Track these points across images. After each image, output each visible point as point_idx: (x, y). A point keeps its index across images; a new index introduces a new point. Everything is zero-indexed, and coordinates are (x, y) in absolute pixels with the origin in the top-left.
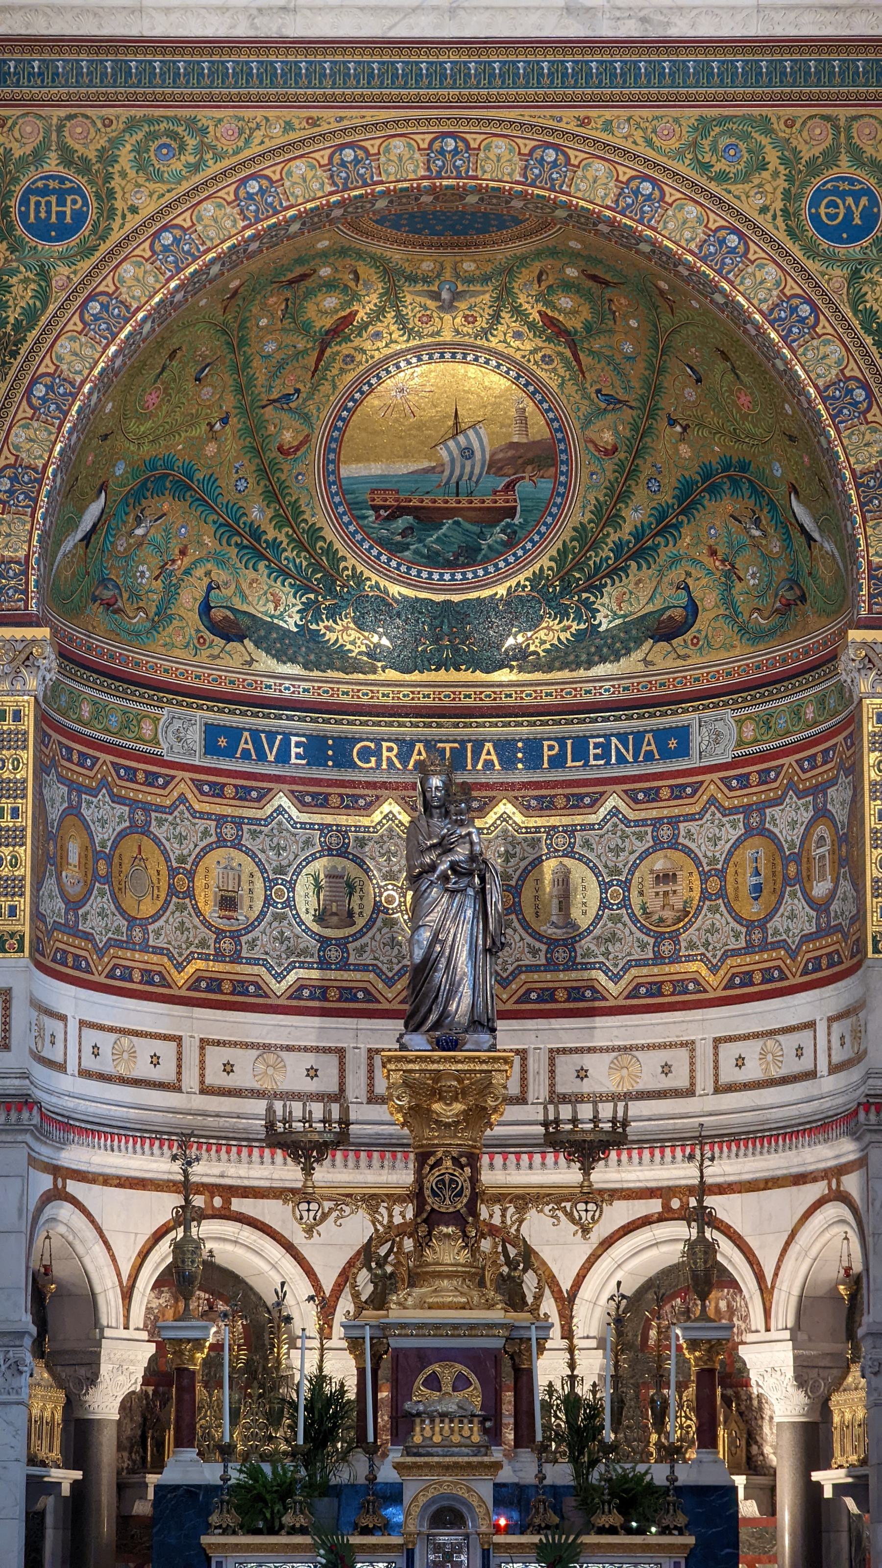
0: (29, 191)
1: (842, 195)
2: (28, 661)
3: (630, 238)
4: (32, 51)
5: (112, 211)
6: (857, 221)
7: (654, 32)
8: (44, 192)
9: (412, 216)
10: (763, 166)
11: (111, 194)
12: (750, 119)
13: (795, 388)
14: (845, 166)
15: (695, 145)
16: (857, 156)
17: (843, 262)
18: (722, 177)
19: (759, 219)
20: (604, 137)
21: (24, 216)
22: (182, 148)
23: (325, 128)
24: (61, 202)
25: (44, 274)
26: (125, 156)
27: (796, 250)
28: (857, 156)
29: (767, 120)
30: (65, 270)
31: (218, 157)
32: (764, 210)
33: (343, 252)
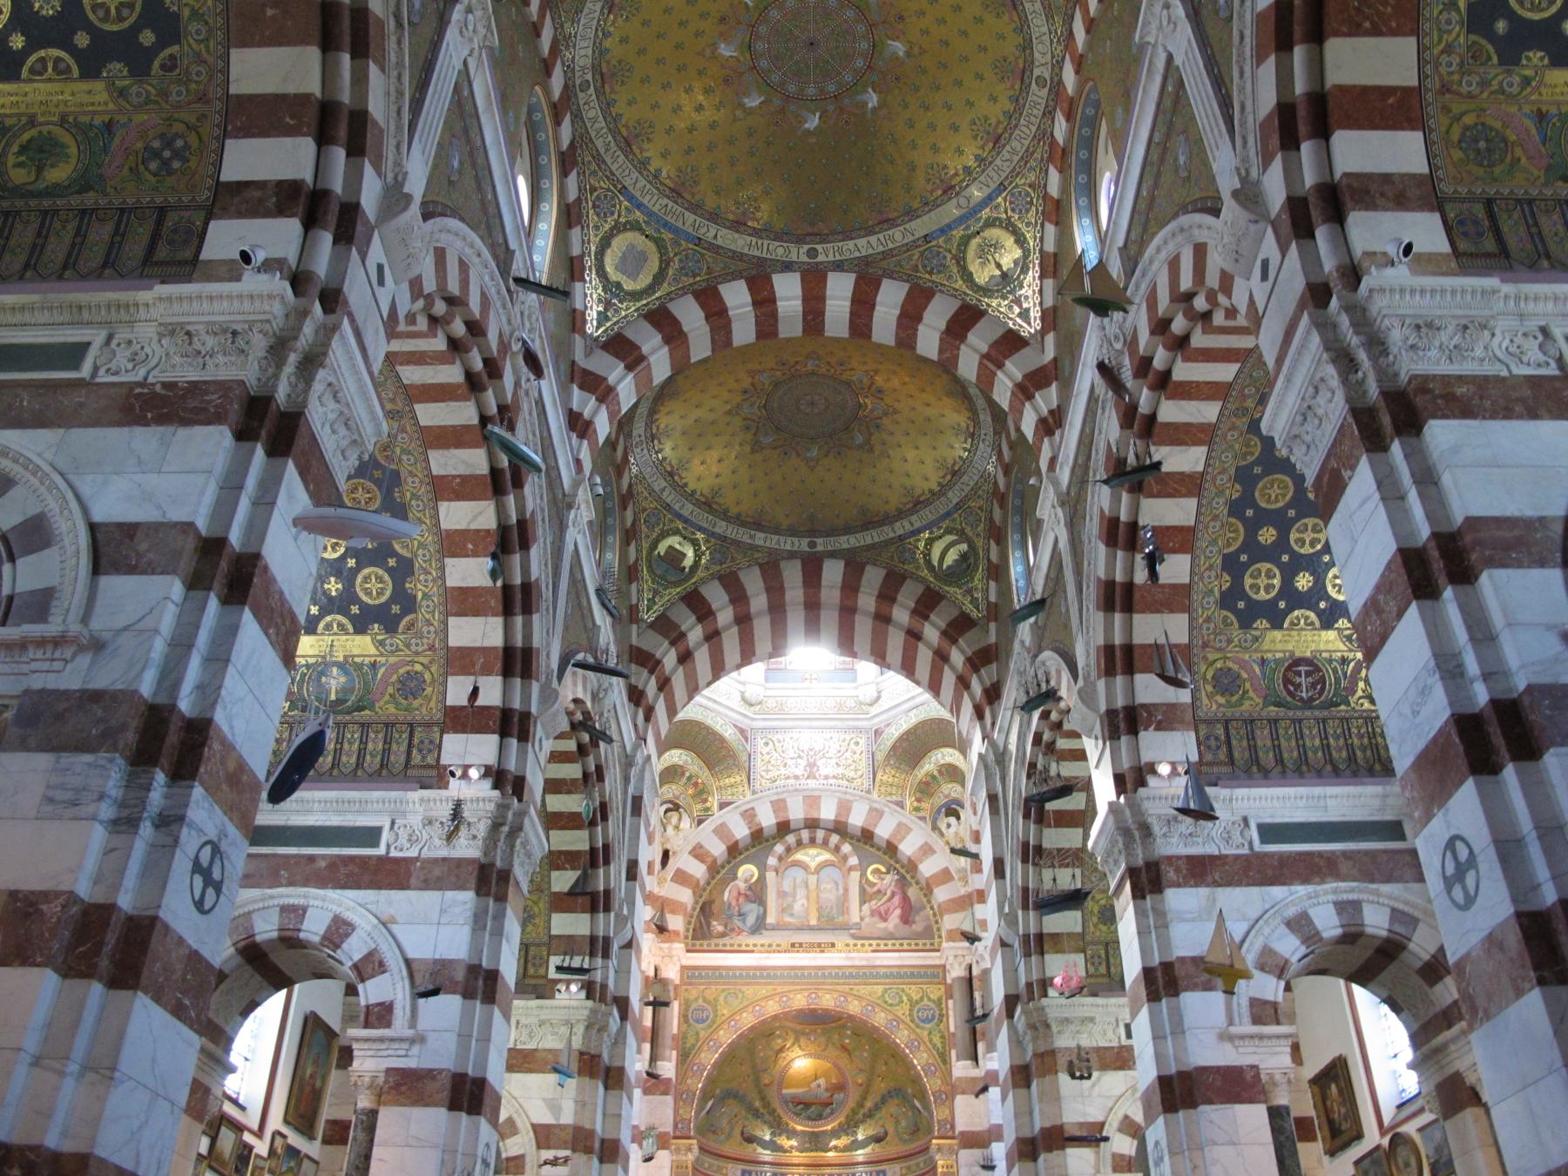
2: (689, 1149)
3: (865, 1023)
13: (914, 1067)
14: (926, 1001)
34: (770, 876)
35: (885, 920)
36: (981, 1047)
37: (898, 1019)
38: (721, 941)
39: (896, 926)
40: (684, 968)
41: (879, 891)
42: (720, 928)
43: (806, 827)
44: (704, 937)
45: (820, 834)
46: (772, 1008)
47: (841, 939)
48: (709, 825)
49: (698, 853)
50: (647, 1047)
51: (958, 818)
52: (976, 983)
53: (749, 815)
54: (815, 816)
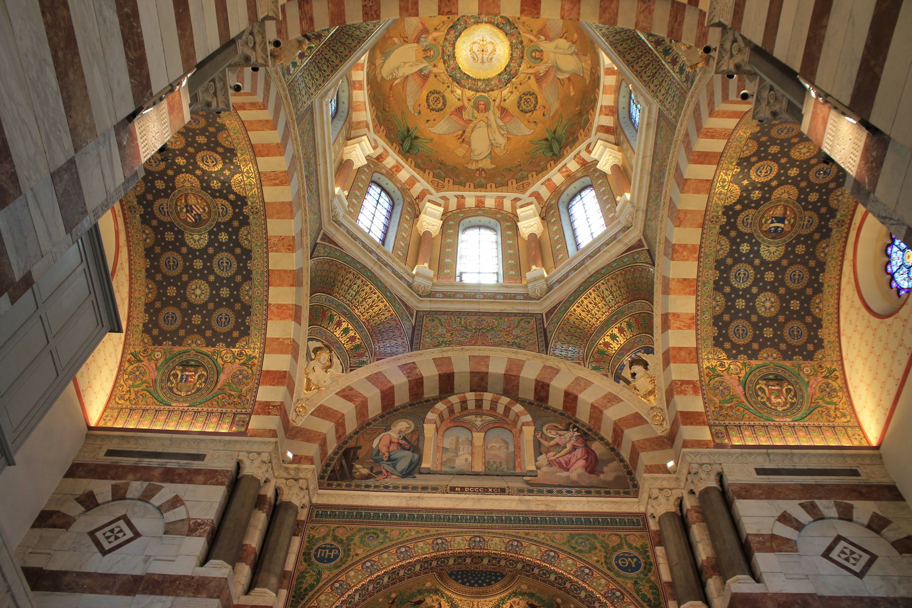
0: (319, 548)
1: (627, 557)
4: (328, 508)
5: (348, 556)
6: (634, 566)
7: (550, 509)
8: (325, 548)
9: (463, 571)
10: (596, 548)
11: (349, 550)
12: (589, 535)
15: (569, 541)
16: (630, 546)
17: (631, 578)
18: (580, 551)
19: (597, 565)
20: (535, 538)
21: (315, 556)
22: (378, 537)
23: (431, 533)
24: (330, 551)
25: (319, 573)
26: (357, 539)
27: (612, 574)
28: (630, 546)
29: (595, 535)
30: (328, 573)
31: (391, 540)
32: (597, 561)
33: (436, 591)
34: (429, 429)
35: (568, 470)
36: (712, 584)
37: (592, 567)
38: (364, 482)
39: (579, 475)
40: (313, 507)
41: (557, 445)
42: (365, 471)
43: (471, 391)
44: (343, 477)
45: (488, 396)
46: (423, 550)
47: (518, 484)
48: (362, 373)
49: (347, 394)
50: (245, 570)
51: (645, 365)
52: (692, 516)
53: (409, 368)
54: (484, 370)
